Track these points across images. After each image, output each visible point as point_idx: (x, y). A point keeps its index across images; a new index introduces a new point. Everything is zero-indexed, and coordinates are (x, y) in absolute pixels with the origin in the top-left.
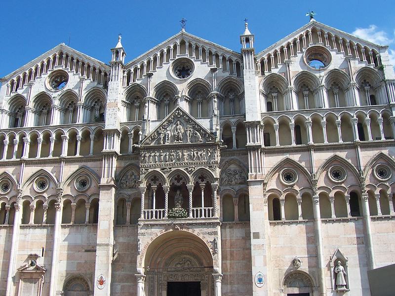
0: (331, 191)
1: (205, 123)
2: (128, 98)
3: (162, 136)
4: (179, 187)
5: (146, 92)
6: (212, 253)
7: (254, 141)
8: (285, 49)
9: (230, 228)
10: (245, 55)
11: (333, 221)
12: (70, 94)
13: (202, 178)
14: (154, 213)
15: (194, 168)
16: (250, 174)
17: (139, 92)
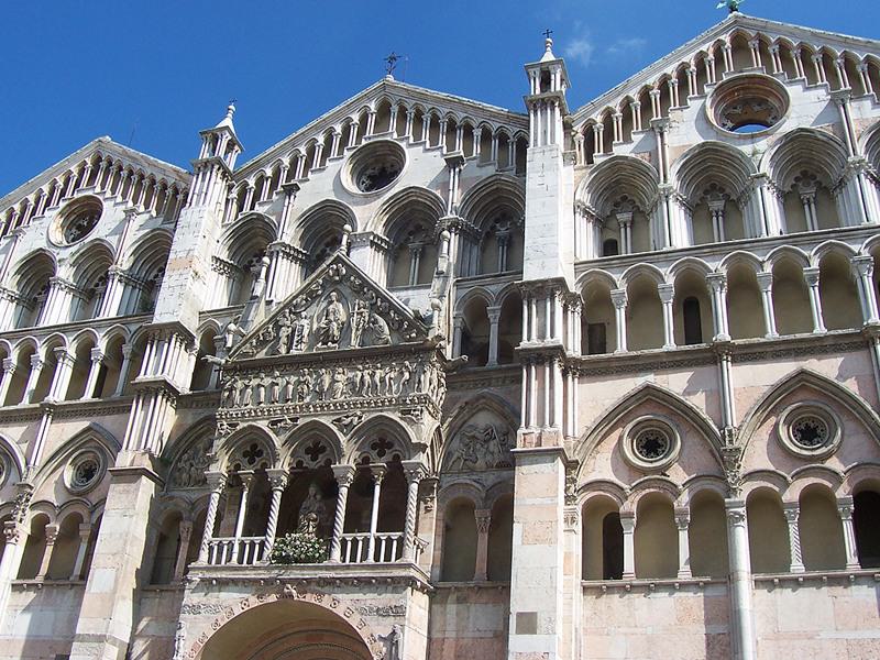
0: (787, 485)
1: (417, 301)
2: (234, 250)
3: (284, 332)
4: (313, 482)
7: (542, 337)
8: (655, 93)
9: (459, 601)
10: (535, 112)
11: (796, 583)
12: (101, 252)
13: (381, 446)
14: (236, 549)
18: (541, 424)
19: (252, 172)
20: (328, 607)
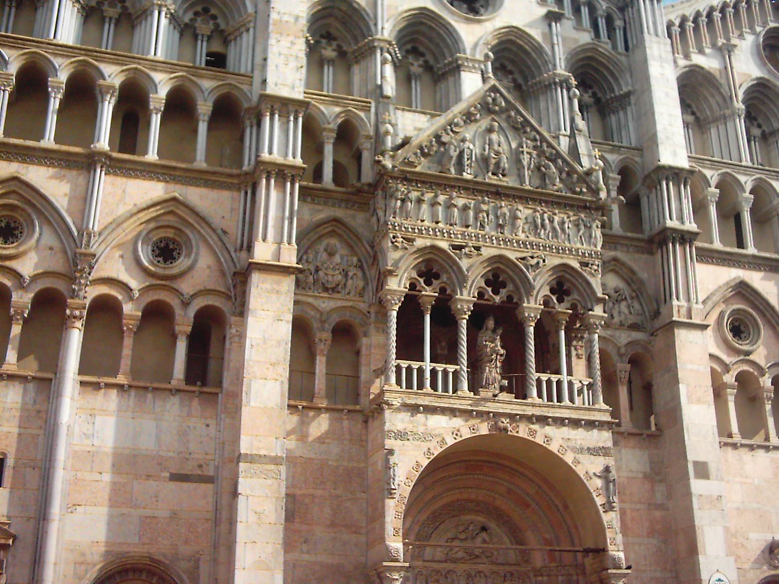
5: (371, 24)
6: (601, 509)
14: (428, 375)
15: (544, 261)
16: (675, 302)
18: (689, 300)
20: (541, 443)
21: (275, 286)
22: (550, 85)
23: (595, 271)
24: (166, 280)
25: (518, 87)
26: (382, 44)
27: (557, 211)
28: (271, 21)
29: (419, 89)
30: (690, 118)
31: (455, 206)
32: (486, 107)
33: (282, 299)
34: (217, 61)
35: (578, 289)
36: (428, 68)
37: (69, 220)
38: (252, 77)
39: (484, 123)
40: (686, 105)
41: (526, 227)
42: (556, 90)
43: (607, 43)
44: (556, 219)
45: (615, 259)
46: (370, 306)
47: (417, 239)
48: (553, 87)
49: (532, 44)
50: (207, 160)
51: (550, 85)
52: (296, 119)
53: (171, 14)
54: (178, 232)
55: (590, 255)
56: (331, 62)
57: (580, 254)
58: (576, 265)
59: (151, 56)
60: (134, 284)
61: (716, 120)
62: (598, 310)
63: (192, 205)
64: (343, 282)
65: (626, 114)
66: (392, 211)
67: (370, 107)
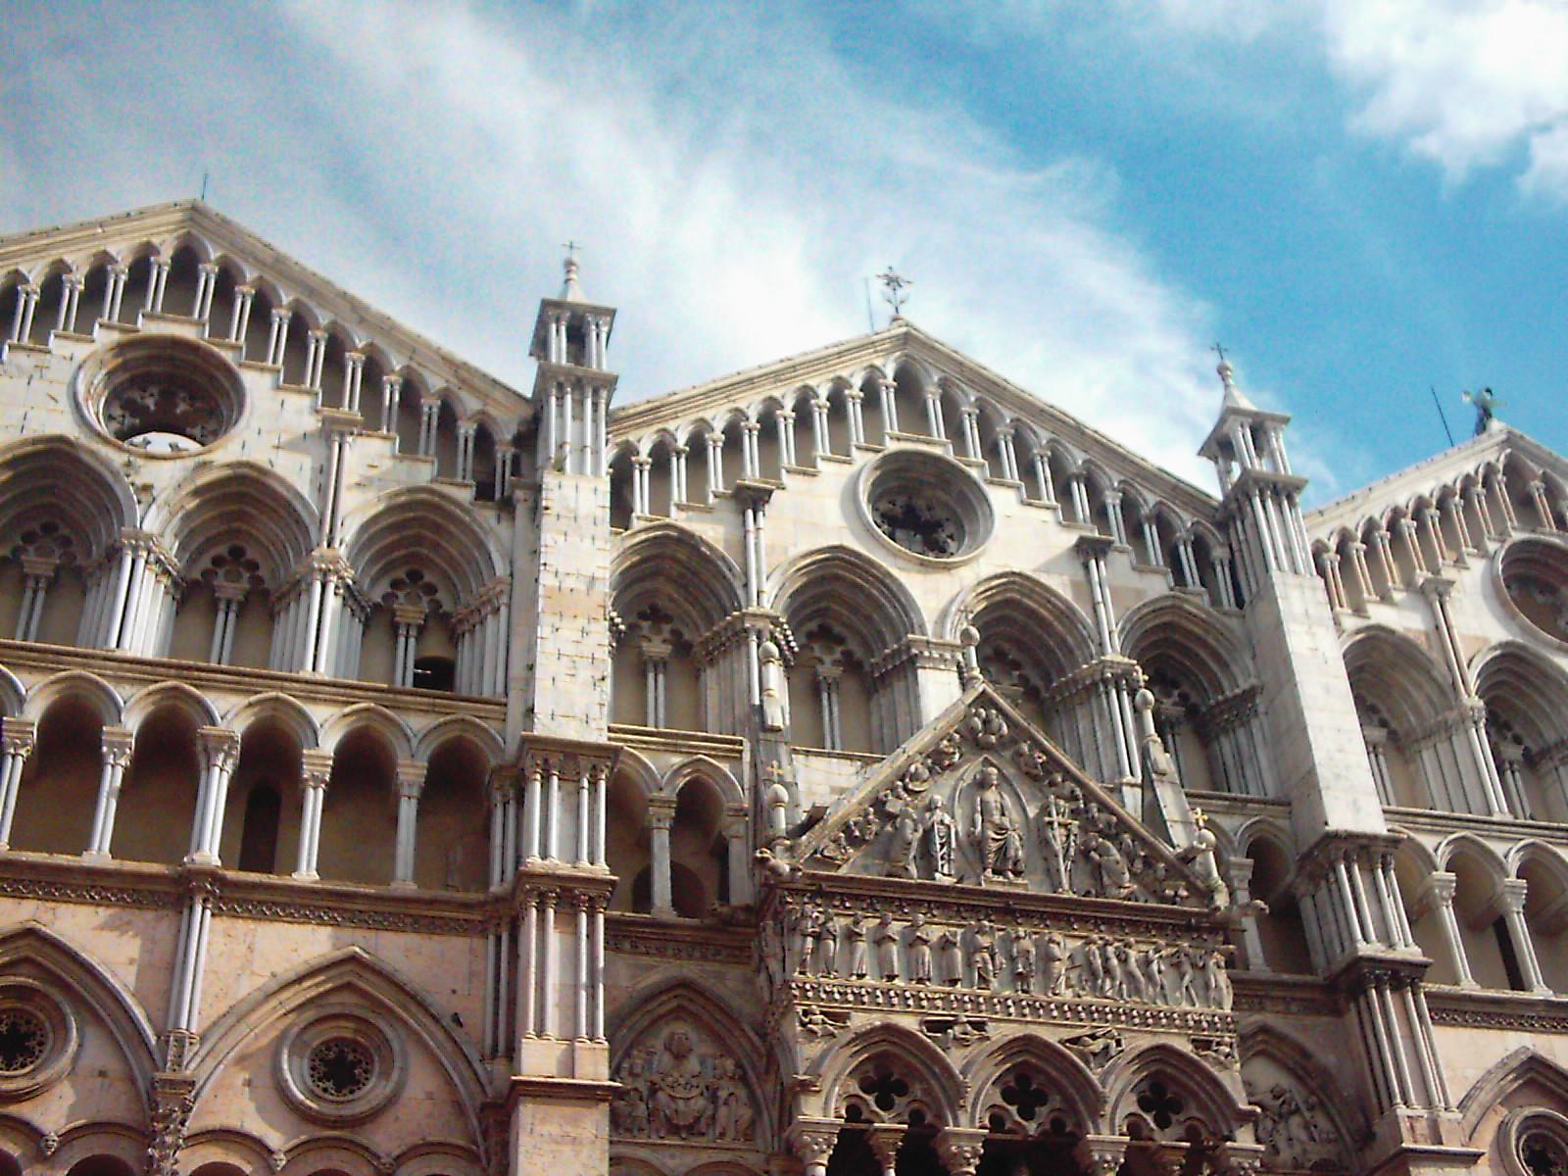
5: (737, 585)
15: (1118, 1043)
16: (1402, 1111)
17: (682, 583)
18: (1429, 1104)
19: (638, 426)
21: (569, 1129)
22: (1095, 684)
23: (1227, 1055)
24: (342, 1128)
25: (1032, 694)
26: (760, 624)
27: (1132, 940)
28: (541, 591)
29: (835, 709)
30: (1379, 734)
31: (926, 942)
32: (970, 738)
33: (583, 1156)
34: (437, 676)
35: (1195, 1095)
36: (851, 664)
37: (138, 1012)
38: (506, 705)
39: (970, 770)
40: (1366, 709)
41: (1073, 975)
42: (1108, 694)
43: (1200, 594)
44: (1133, 954)
45: (1264, 1029)
46: (768, 1161)
47: (853, 1014)
48: (1102, 689)
49: (1054, 605)
50: (418, 876)
51: (1095, 684)
52: (594, 784)
53: (348, 587)
54: (363, 1027)
55: (1211, 1023)
56: (660, 665)
57: (1191, 1023)
58: (1185, 1047)
59: (307, 672)
60: (275, 1139)
61: (1428, 735)
62: (1244, 1138)
63: (388, 969)
64: (709, 1112)
65: (1251, 735)
66: (797, 959)
67: (740, 752)
